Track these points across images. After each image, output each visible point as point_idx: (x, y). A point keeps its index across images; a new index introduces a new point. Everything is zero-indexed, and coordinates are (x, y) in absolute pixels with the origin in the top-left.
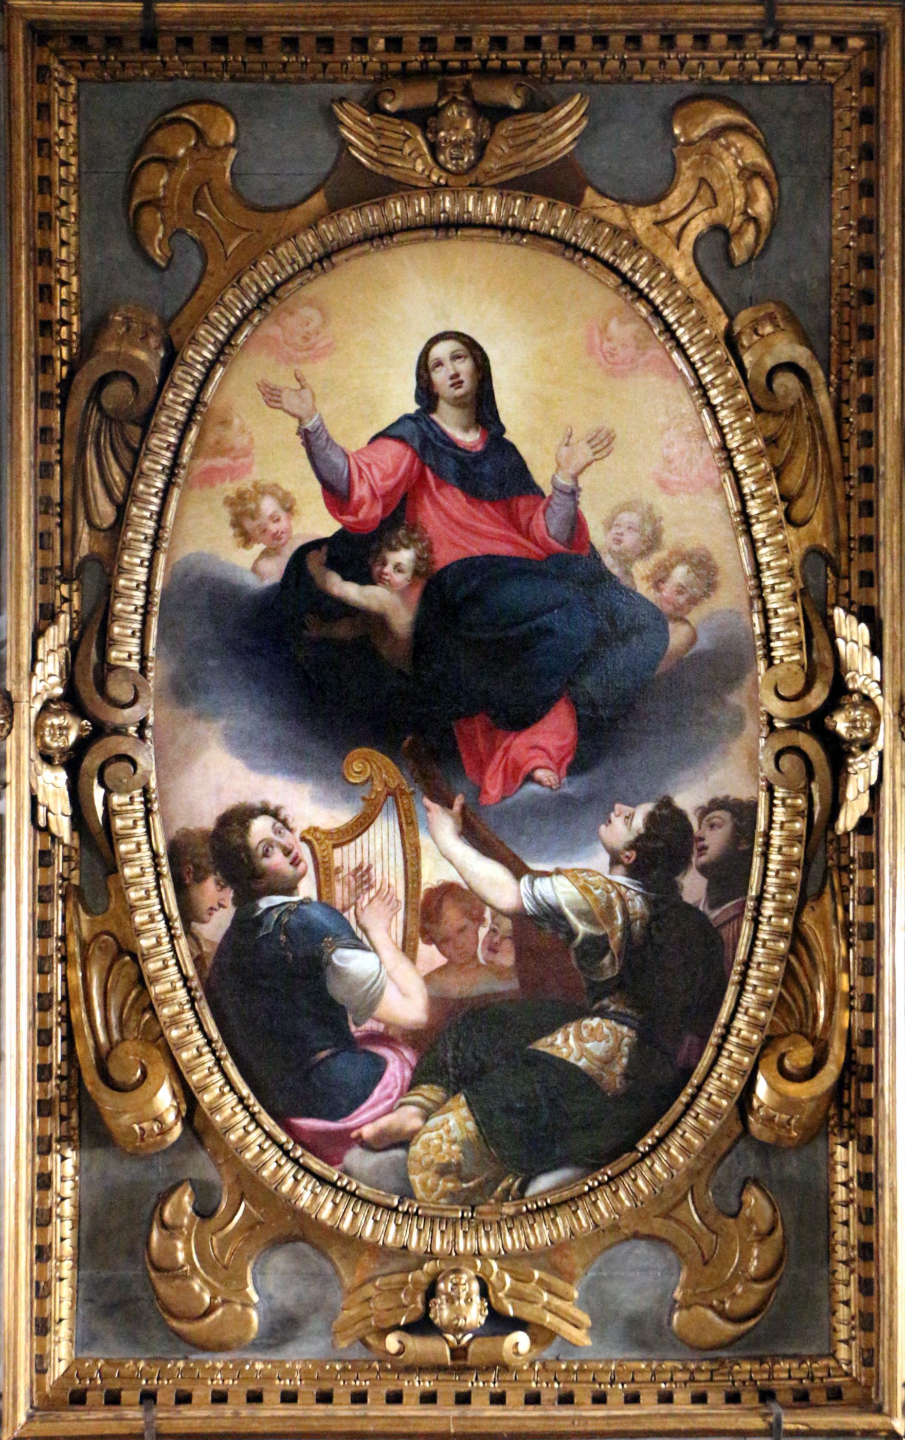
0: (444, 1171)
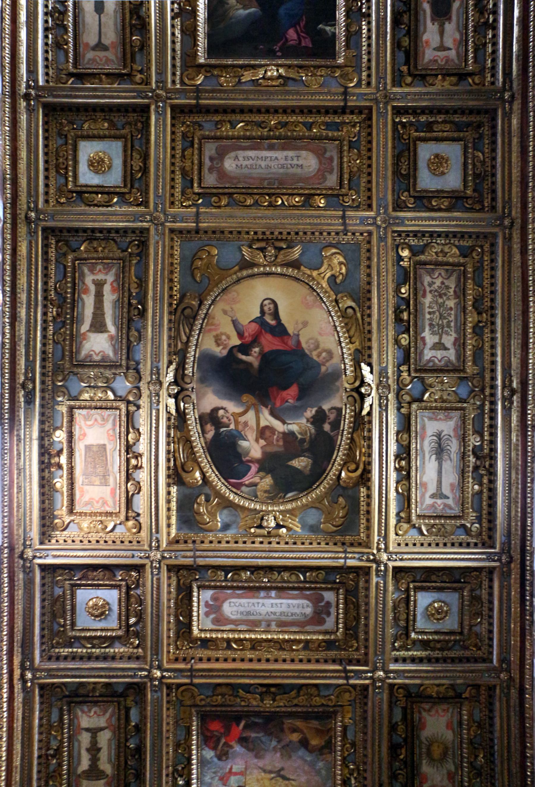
0: (265, 492)
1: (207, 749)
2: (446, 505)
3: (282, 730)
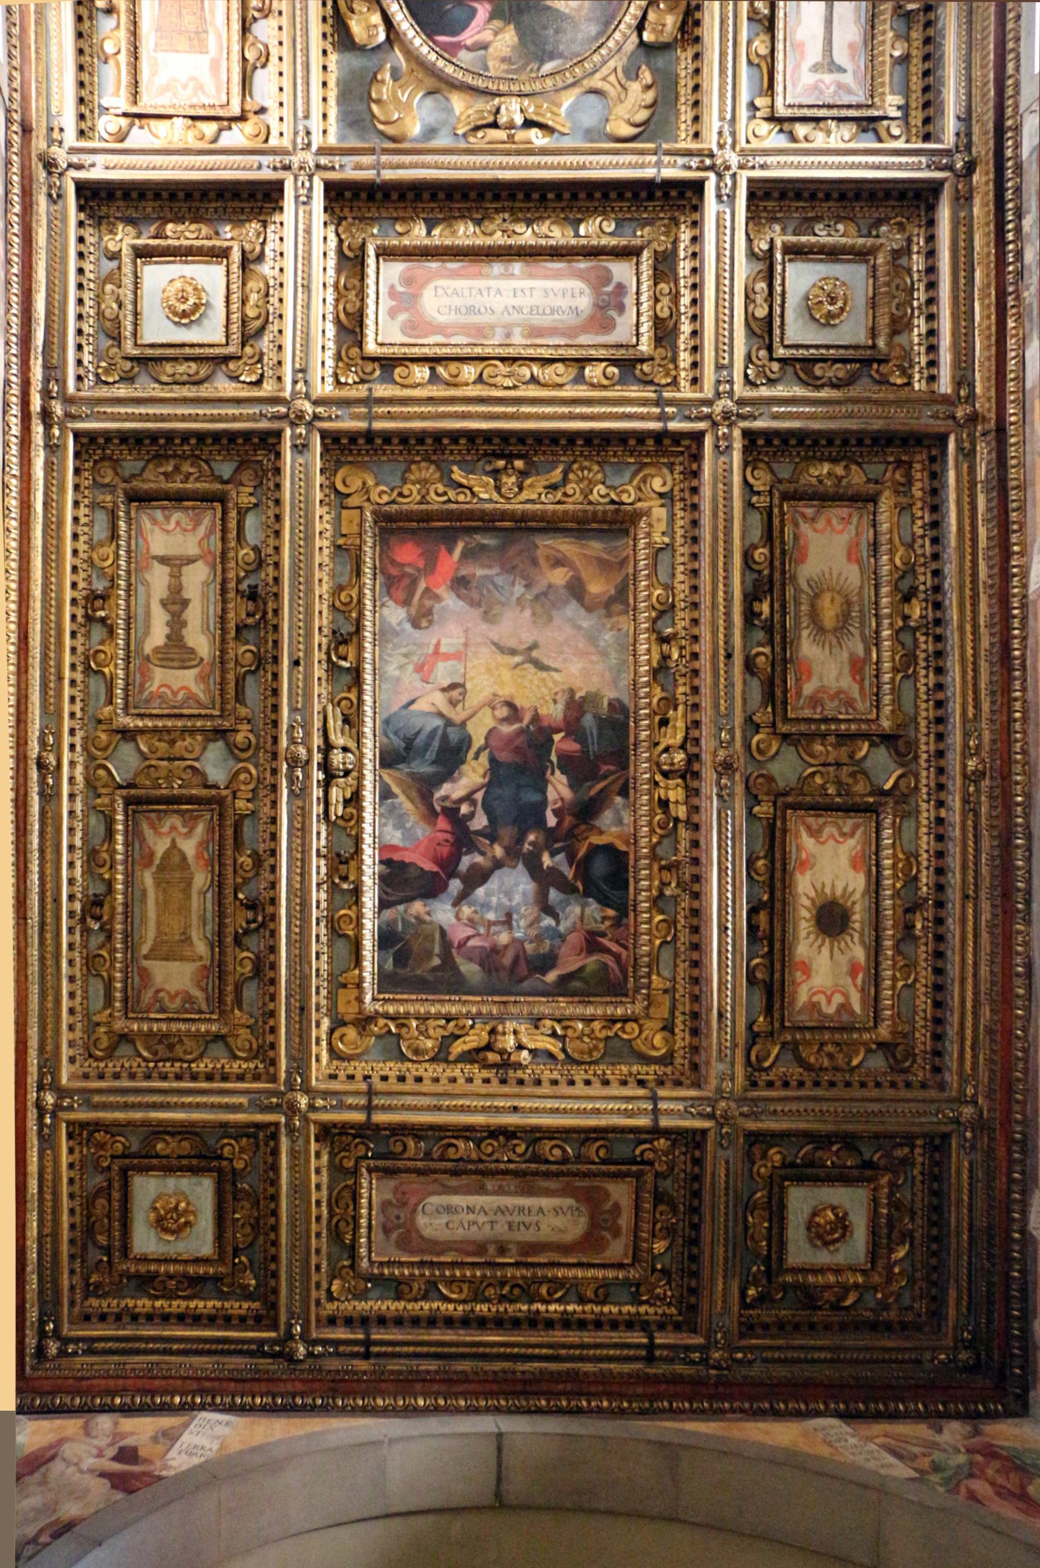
0: (504, 60)
1: (391, 603)
2: (840, 86)
3: (534, 562)
